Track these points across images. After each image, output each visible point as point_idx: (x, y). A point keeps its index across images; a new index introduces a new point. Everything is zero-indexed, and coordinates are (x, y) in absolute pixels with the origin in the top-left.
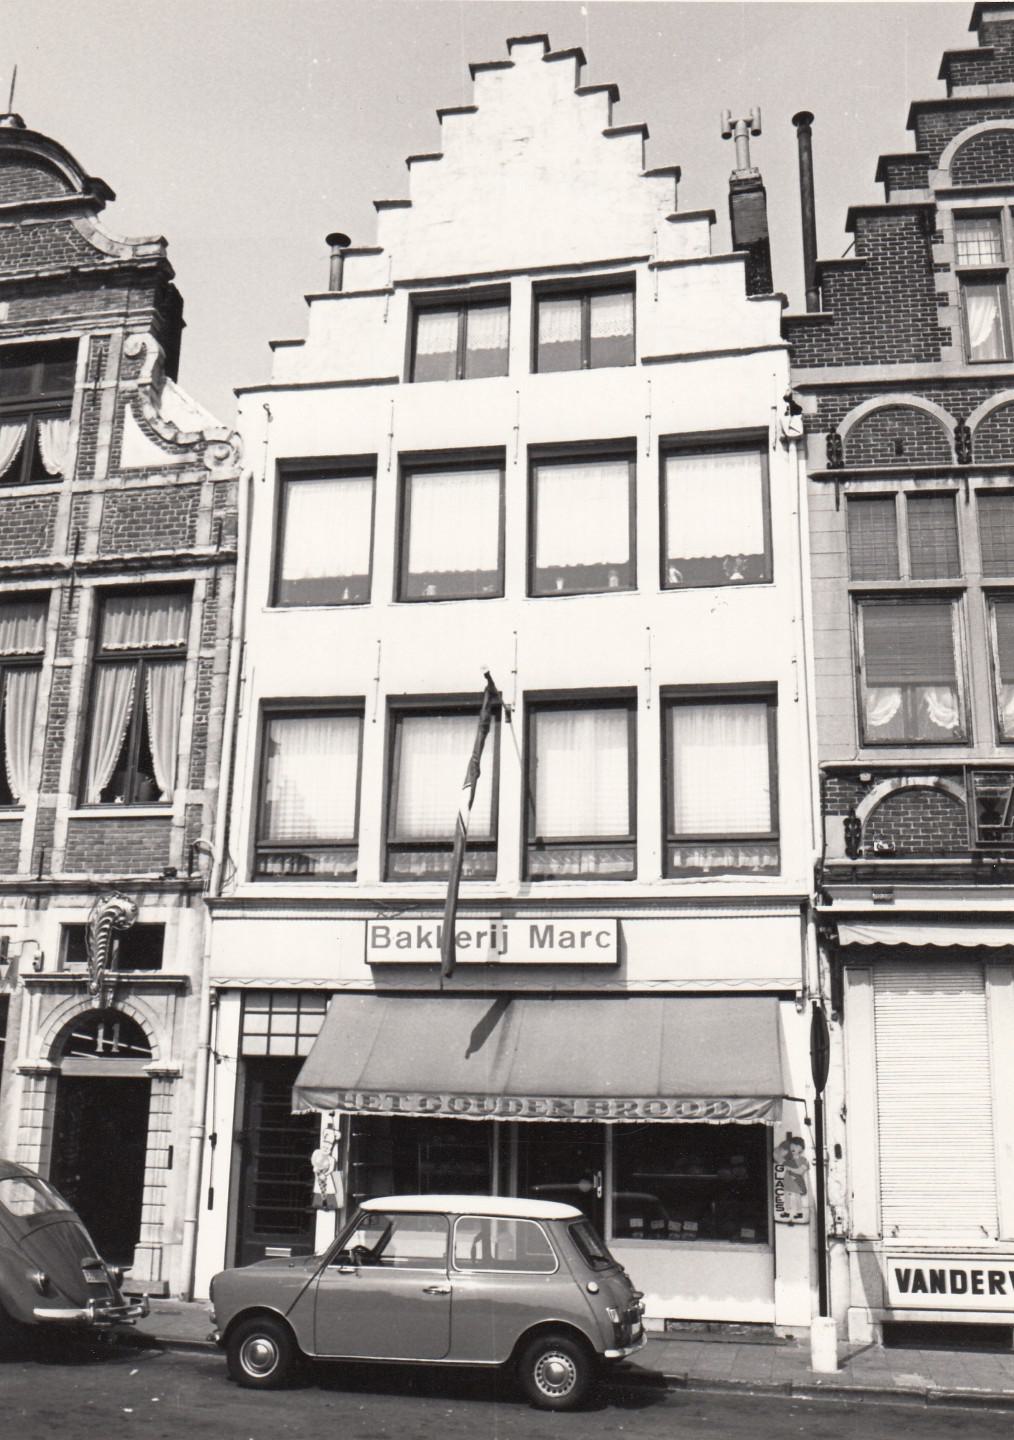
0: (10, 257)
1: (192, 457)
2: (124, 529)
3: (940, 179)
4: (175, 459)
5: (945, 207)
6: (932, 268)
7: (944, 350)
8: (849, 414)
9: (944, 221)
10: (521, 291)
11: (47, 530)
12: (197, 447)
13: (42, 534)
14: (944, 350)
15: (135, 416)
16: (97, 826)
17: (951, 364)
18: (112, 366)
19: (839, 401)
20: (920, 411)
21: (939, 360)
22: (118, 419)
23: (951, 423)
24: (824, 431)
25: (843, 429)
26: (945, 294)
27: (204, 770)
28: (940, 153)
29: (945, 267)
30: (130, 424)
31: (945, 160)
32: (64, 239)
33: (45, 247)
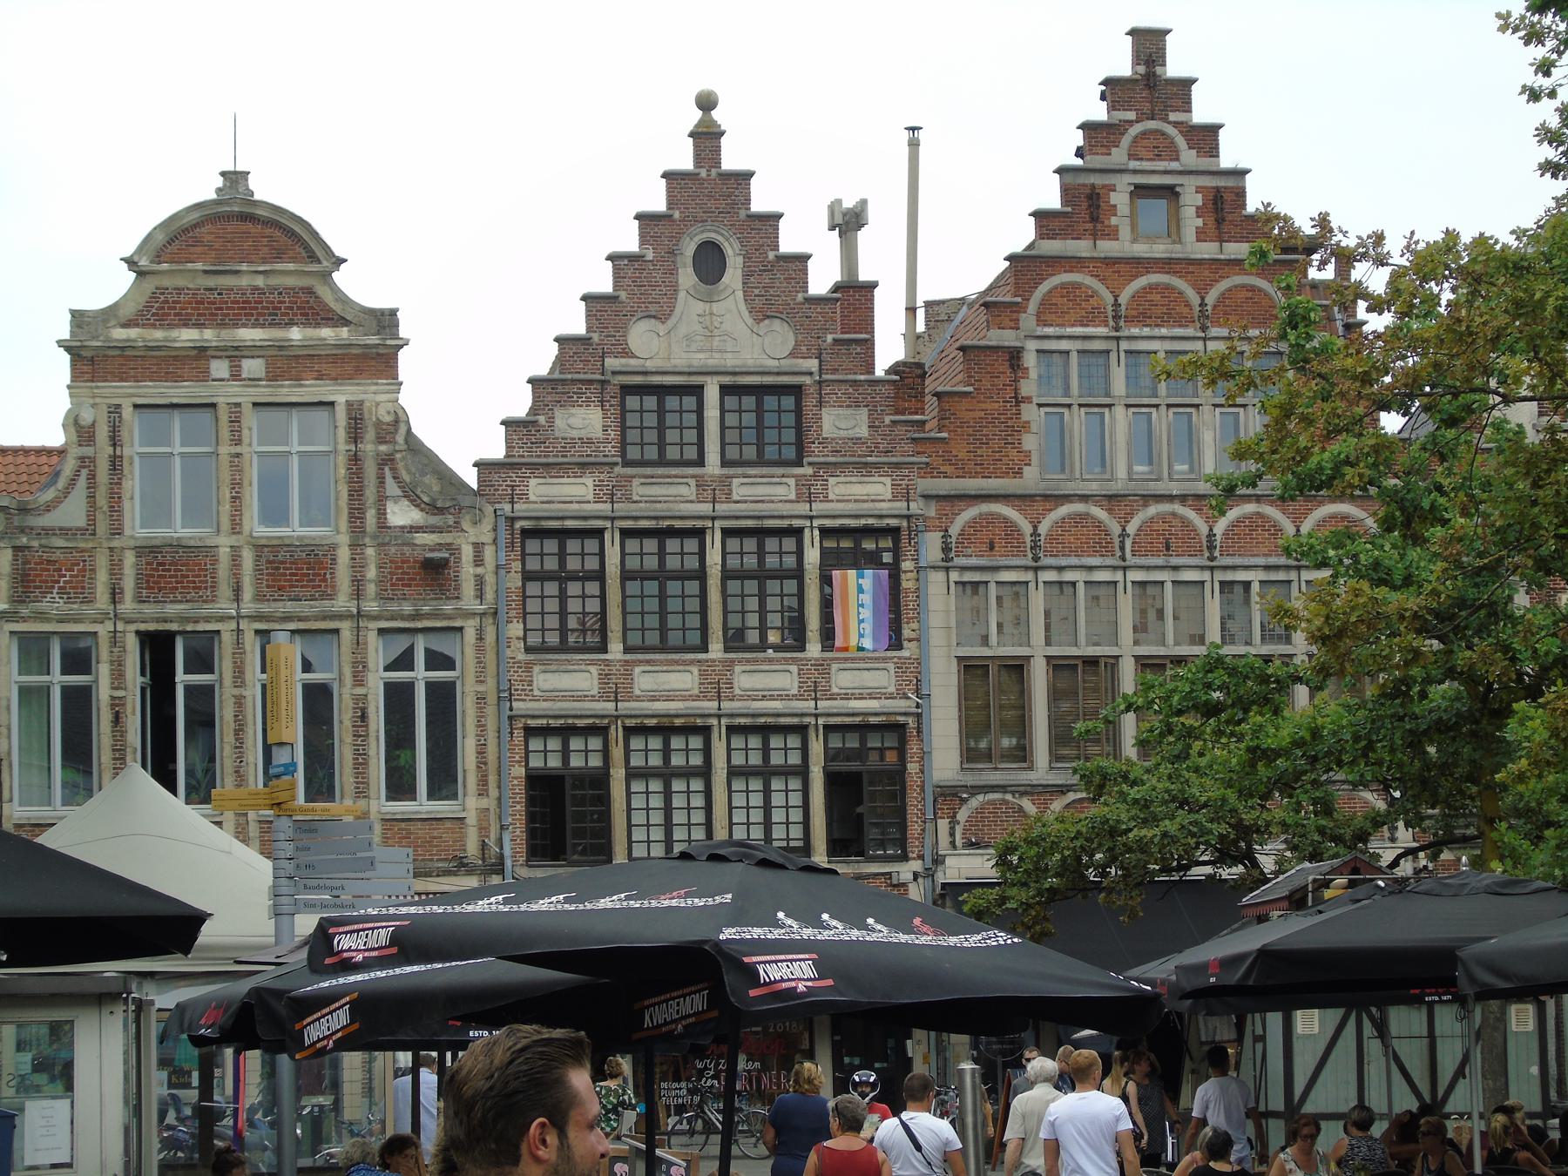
0: (258, 314)
1: (451, 520)
2: (398, 579)
3: (1028, 320)
4: (434, 520)
5: (1032, 346)
6: (1019, 400)
7: (1026, 469)
9: (1030, 360)
10: (712, 394)
11: (328, 576)
12: (452, 510)
13: (325, 580)
14: (1026, 469)
15: (394, 478)
16: (403, 825)
17: (1031, 479)
18: (370, 434)
20: (1006, 520)
22: (381, 481)
23: (1027, 528)
25: (954, 531)
26: (1029, 422)
27: (486, 781)
29: (1028, 400)
30: (389, 480)
31: (1032, 307)
32: (308, 302)
33: (292, 308)
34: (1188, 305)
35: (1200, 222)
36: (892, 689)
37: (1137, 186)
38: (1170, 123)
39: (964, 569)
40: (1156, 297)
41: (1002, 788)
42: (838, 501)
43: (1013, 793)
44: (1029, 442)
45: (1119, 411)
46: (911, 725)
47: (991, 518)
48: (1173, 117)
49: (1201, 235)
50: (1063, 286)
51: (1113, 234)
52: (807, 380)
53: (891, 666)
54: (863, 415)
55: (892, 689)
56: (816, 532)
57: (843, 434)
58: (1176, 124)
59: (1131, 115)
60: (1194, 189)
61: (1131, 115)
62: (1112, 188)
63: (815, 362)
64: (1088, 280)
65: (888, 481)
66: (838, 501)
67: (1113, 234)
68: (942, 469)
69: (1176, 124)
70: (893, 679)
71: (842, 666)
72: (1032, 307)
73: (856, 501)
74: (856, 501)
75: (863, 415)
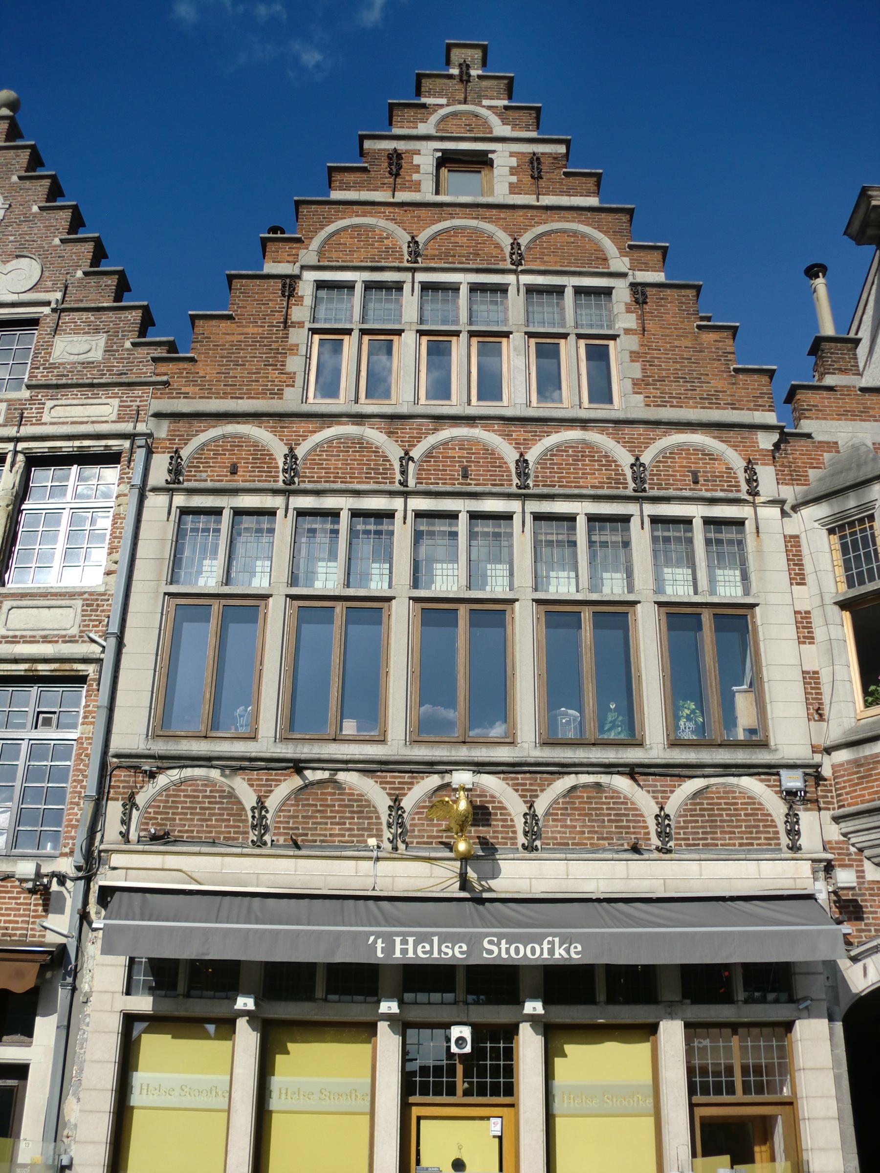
5: (310, 276)
8: (195, 439)
19: (182, 425)
21: (281, 398)
24: (169, 452)
28: (312, 238)
31: (315, 244)
34: (498, 246)
35: (514, 179)
36: (74, 631)
37: (444, 151)
38: (484, 106)
39: (191, 491)
40: (461, 240)
41: (207, 761)
42: (52, 424)
43: (222, 768)
44: (294, 364)
45: (409, 338)
46: (92, 676)
47: (238, 441)
48: (486, 102)
49: (514, 189)
50: (354, 227)
51: (416, 187)
52: (46, 310)
53: (78, 603)
54: (101, 340)
55: (74, 631)
56: (20, 458)
57: (75, 358)
58: (489, 108)
59: (443, 101)
60: (508, 154)
61: (443, 101)
62: (418, 152)
63: (59, 295)
64: (382, 223)
65: (116, 402)
66: (52, 424)
67: (416, 187)
68: (184, 390)
69: (489, 108)
70: (79, 618)
71: (15, 603)
72: (315, 244)
73: (73, 423)
74: (73, 423)
75: (101, 340)
